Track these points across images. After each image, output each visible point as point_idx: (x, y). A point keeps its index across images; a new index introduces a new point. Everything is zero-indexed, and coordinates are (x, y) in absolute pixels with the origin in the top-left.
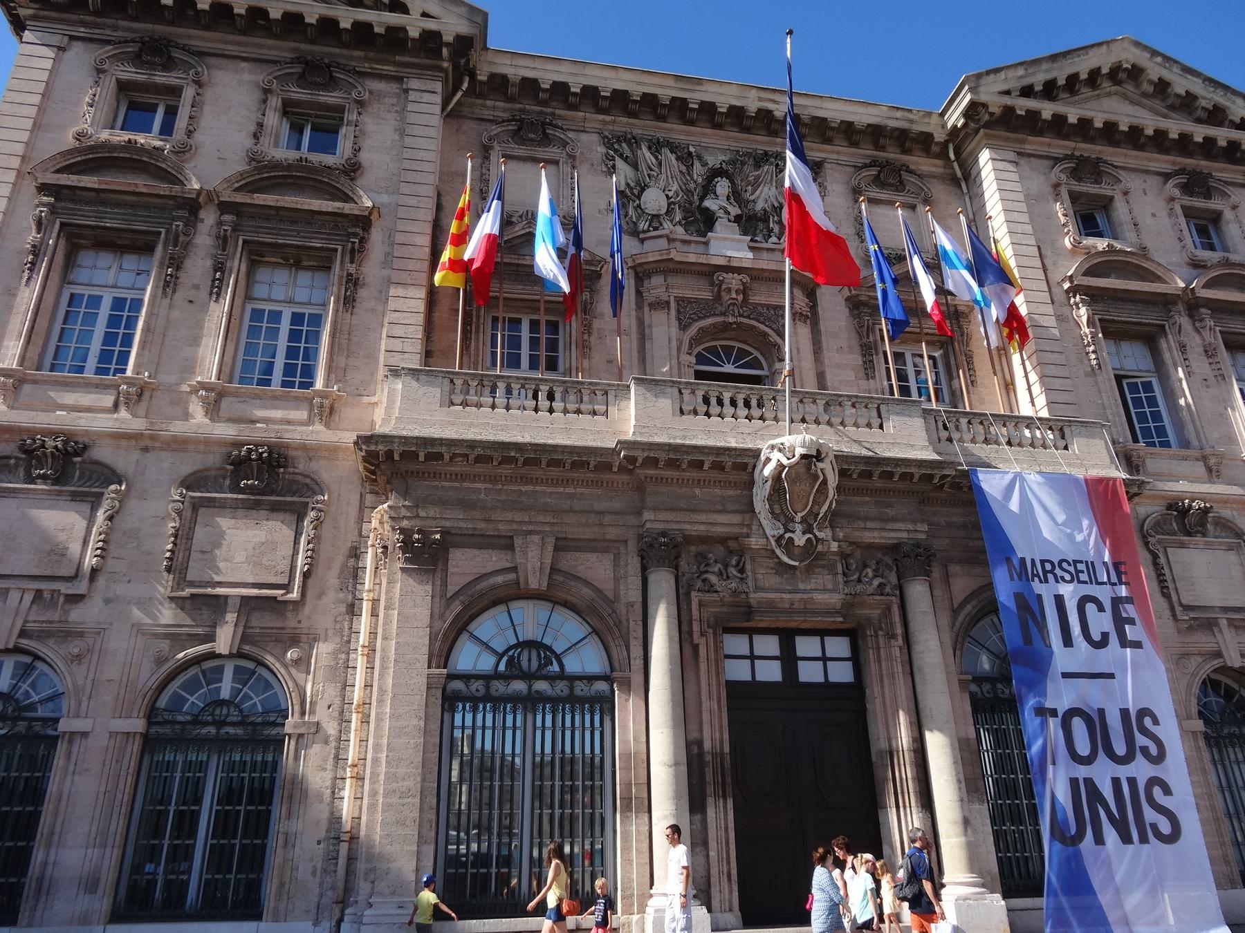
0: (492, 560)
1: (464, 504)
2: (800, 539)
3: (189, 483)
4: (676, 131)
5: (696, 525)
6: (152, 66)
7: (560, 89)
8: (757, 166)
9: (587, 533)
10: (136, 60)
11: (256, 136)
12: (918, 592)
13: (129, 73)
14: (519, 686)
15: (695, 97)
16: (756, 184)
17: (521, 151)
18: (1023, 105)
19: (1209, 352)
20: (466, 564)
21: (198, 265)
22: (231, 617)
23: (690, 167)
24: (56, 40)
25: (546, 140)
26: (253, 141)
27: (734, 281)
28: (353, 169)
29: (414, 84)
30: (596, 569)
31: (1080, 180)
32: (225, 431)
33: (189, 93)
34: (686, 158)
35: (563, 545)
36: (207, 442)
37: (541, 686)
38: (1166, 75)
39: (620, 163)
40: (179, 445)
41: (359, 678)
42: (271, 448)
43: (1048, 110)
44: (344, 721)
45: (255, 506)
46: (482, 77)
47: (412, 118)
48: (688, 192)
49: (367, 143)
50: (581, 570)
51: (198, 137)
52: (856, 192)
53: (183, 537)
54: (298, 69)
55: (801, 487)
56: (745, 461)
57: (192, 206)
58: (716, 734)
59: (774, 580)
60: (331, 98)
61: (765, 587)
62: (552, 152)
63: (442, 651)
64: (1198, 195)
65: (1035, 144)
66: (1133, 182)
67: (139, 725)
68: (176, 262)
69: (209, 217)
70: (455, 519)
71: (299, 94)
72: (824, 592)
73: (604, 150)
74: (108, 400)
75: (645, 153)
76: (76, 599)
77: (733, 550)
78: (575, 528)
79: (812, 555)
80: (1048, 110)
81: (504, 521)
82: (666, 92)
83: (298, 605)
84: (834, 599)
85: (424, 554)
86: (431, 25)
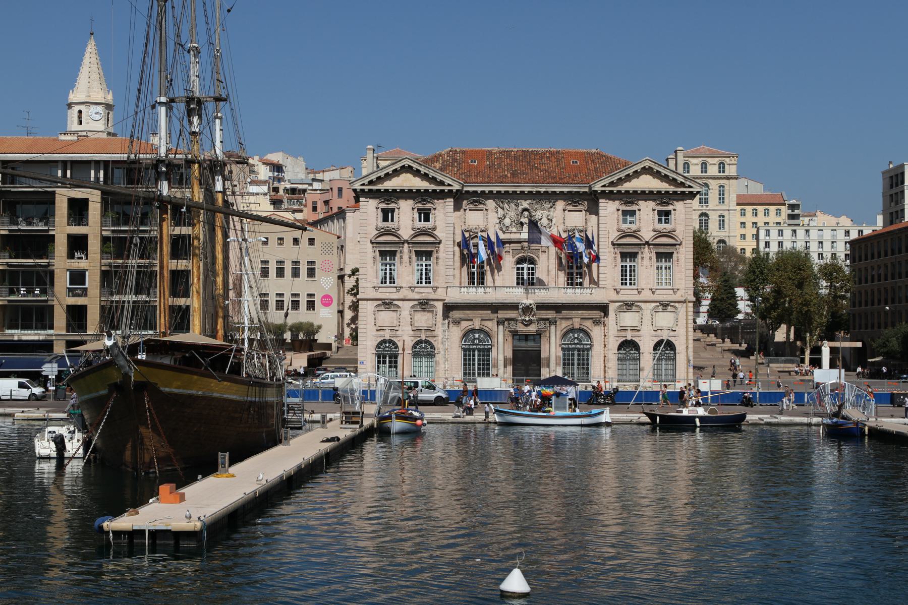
0: (469, 323)
2: (527, 319)
3: (413, 307)
5: (508, 316)
7: (483, 192)
12: (553, 328)
16: (536, 210)
18: (607, 189)
19: (651, 259)
20: (464, 324)
28: (434, 229)
29: (448, 200)
32: (417, 297)
34: (517, 205)
39: (499, 209)
43: (615, 189)
52: (564, 210)
60: (428, 206)
61: (521, 328)
62: (481, 207)
65: (613, 197)
68: (401, 257)
69: (406, 245)
75: (506, 206)
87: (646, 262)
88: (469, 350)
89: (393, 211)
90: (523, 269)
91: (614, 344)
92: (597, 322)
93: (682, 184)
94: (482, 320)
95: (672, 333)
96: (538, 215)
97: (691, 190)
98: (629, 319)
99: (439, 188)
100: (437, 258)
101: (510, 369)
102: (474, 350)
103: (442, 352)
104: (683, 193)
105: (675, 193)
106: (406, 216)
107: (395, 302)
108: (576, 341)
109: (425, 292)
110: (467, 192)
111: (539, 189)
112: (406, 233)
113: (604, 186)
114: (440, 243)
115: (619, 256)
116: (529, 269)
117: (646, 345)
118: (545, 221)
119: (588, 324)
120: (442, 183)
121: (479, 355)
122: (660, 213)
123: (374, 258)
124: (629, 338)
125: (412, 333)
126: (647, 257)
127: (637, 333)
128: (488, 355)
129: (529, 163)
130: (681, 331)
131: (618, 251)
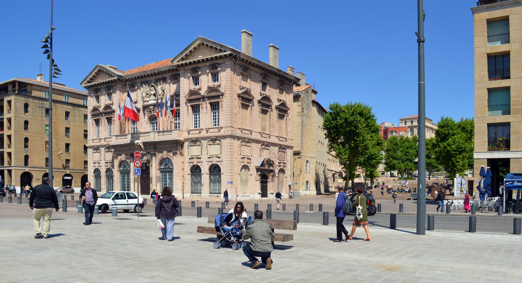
4: (148, 79)
12: (154, 158)
15: (146, 74)
68: (101, 122)
82: (143, 75)
87: (204, 110)
95: (218, 159)
97: (225, 53)
98: (195, 150)
104: (221, 56)
113: (178, 61)
114: (114, 112)
115: (190, 109)
117: (205, 169)
124: (195, 164)
126: (205, 107)
127: (199, 160)
130: (224, 157)
131: (189, 105)
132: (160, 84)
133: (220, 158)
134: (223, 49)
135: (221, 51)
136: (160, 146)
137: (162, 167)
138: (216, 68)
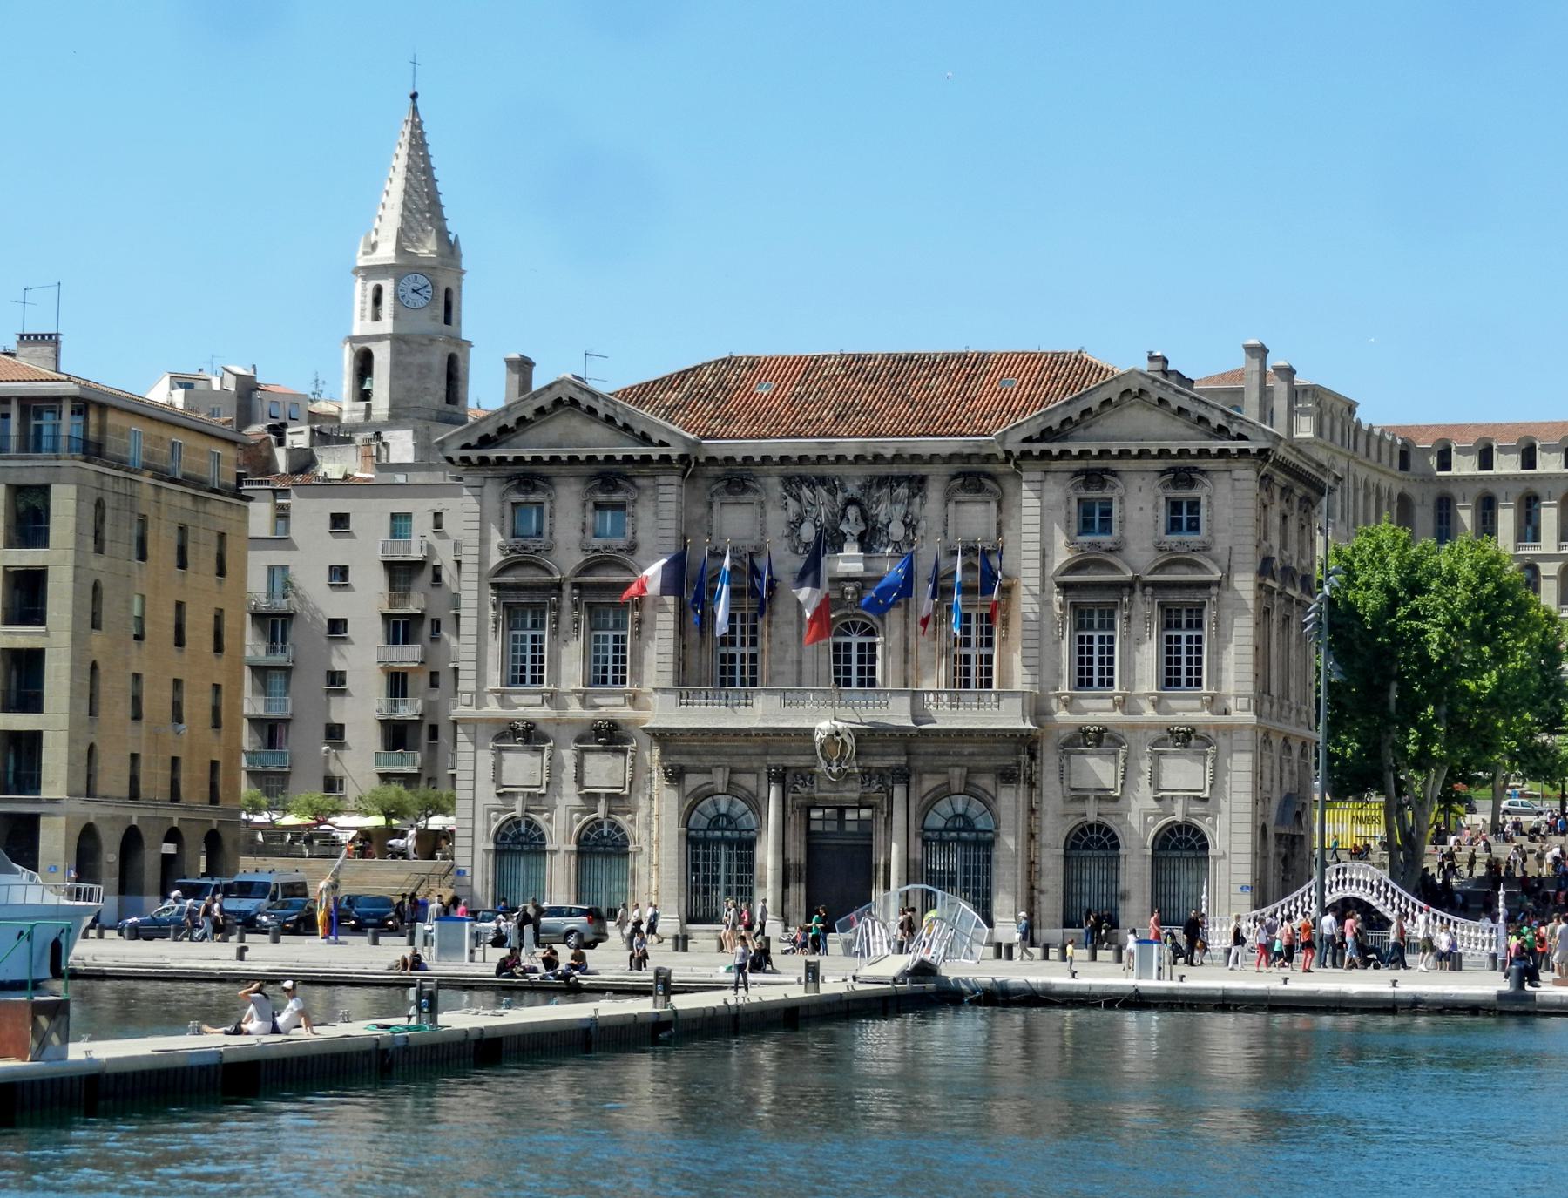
1: (690, 754)
3: (579, 740)
5: (791, 762)
6: (527, 492)
8: (879, 487)
9: (744, 765)
10: (518, 489)
11: (583, 531)
12: (899, 792)
13: (517, 497)
14: (718, 834)
16: (878, 502)
17: (731, 499)
18: (1037, 448)
20: (692, 781)
21: (566, 618)
22: (603, 801)
23: (835, 497)
24: (477, 482)
25: (745, 489)
26: (579, 535)
27: (850, 588)
29: (662, 480)
30: (749, 781)
31: (1087, 489)
32: (590, 714)
33: (547, 507)
34: (832, 492)
35: (733, 771)
36: (583, 721)
37: (728, 833)
38: (1164, 395)
39: (790, 501)
40: (571, 722)
41: (655, 828)
42: (610, 722)
44: (651, 846)
45: (605, 751)
46: (702, 460)
47: (663, 506)
48: (834, 515)
49: (640, 525)
50: (742, 783)
51: (556, 536)
53: (579, 766)
54: (598, 482)
55: (832, 747)
56: (810, 732)
57: (558, 586)
58: (797, 854)
59: (828, 787)
61: (823, 791)
62: (748, 497)
63: (686, 821)
64: (1181, 487)
65: (1055, 465)
66: (1136, 481)
67: (573, 847)
68: (556, 620)
69: (567, 588)
70: (686, 761)
71: (601, 497)
72: (851, 792)
73: (780, 489)
74: (538, 699)
75: (806, 492)
76: (542, 795)
77: (807, 775)
78: (738, 762)
79: (845, 776)
80: (1055, 449)
81: (708, 761)
83: (628, 796)
84: (856, 796)
85: (675, 776)
86: (664, 451)
88: (706, 843)
89: (539, 506)
90: (848, 646)
91: (1054, 833)
92: (1007, 777)
93: (1221, 431)
94: (733, 771)
95: (1197, 808)
96: (882, 511)
97: (1243, 445)
99: (638, 451)
100: (639, 621)
101: (798, 892)
102: (717, 841)
103: (646, 849)
105: (1203, 453)
106: (568, 527)
107: (541, 727)
108: (960, 823)
109: (611, 706)
110: (711, 460)
111: (882, 451)
112: (567, 559)
113: (1028, 440)
116: (861, 647)
118: (897, 531)
119: (986, 781)
120: (645, 439)
121: (729, 858)
122: (1175, 506)
123: (496, 621)
124: (1092, 818)
125: (577, 801)
127: (1111, 806)
128: (751, 858)
129: (893, 388)
132: (894, 502)
133: (1206, 800)
134: (1235, 429)
135: (1221, 431)
136: (931, 748)
137: (935, 821)
138: (1191, 484)
